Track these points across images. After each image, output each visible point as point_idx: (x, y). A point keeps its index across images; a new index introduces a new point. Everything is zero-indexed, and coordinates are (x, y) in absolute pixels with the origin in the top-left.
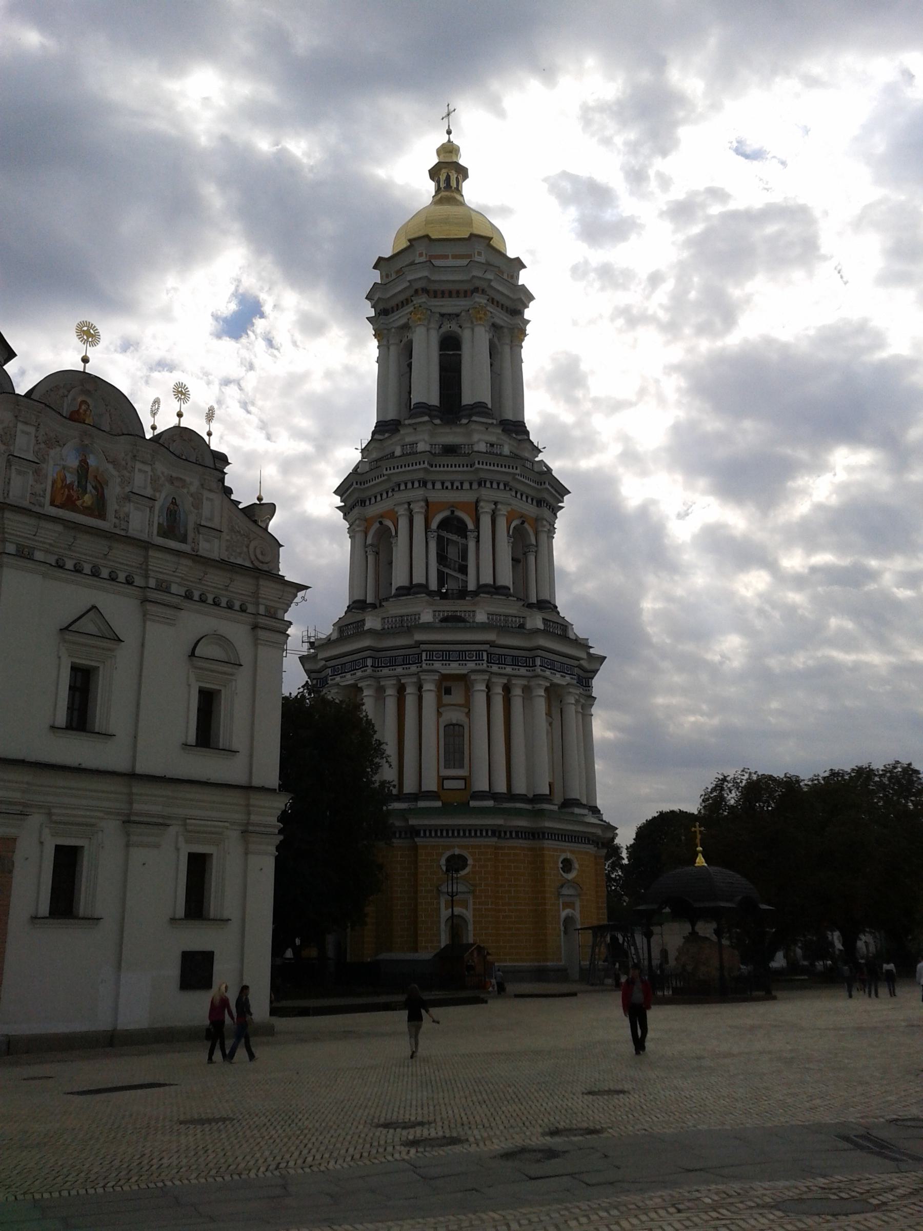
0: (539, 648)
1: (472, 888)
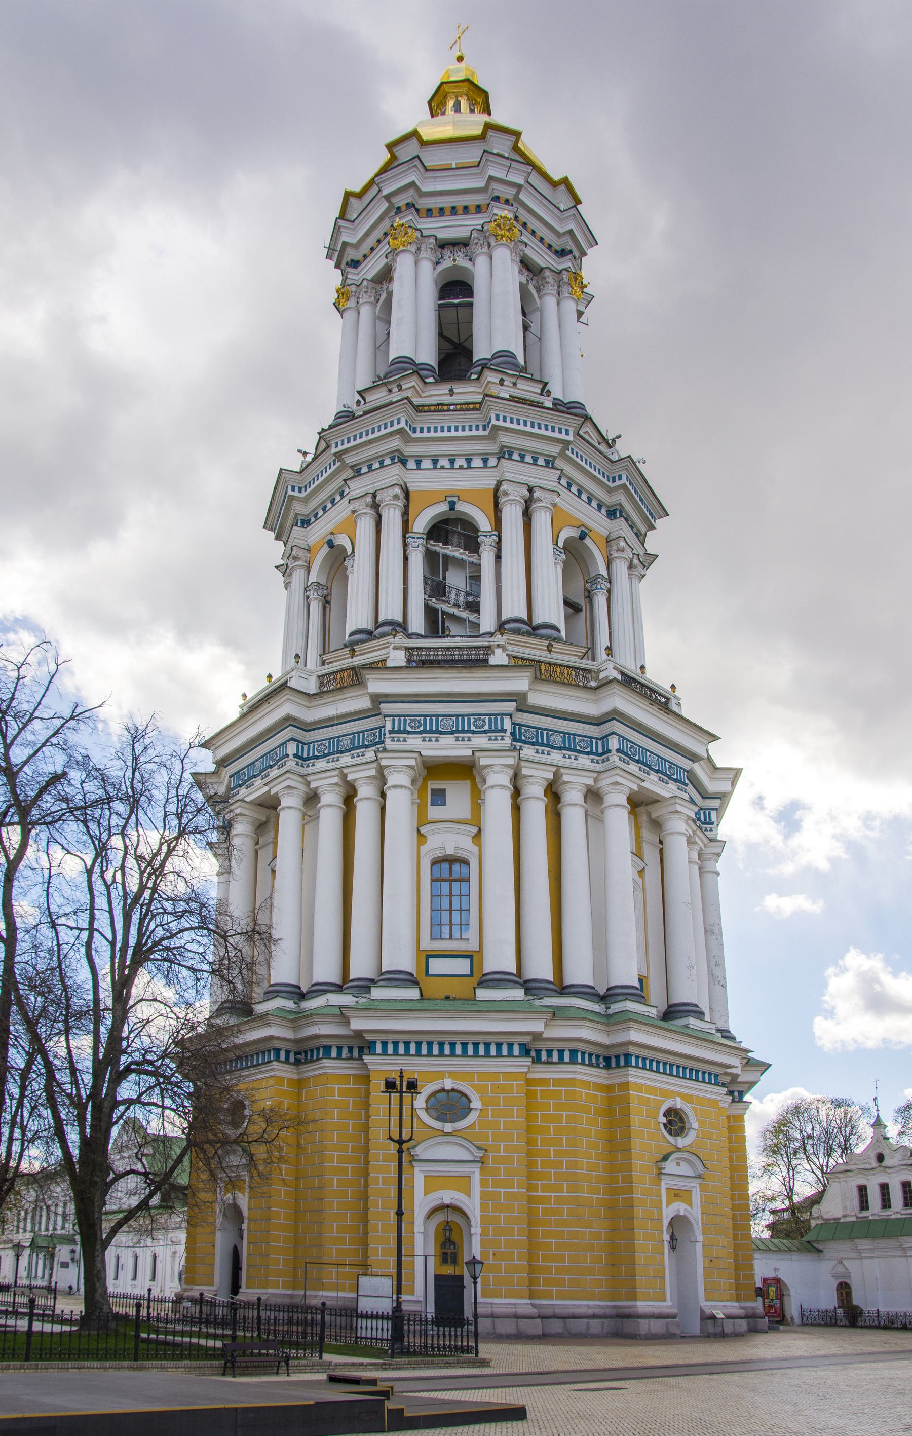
0: (615, 715)
1: (480, 1154)
